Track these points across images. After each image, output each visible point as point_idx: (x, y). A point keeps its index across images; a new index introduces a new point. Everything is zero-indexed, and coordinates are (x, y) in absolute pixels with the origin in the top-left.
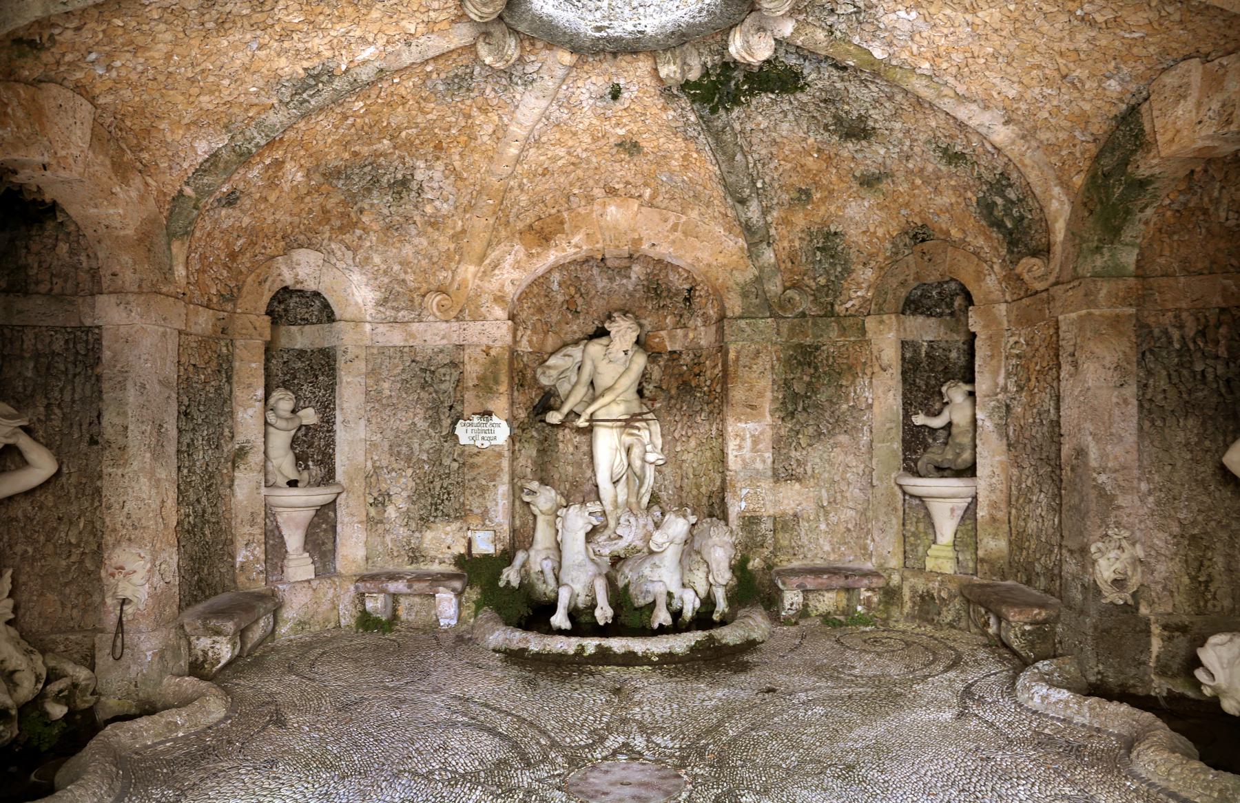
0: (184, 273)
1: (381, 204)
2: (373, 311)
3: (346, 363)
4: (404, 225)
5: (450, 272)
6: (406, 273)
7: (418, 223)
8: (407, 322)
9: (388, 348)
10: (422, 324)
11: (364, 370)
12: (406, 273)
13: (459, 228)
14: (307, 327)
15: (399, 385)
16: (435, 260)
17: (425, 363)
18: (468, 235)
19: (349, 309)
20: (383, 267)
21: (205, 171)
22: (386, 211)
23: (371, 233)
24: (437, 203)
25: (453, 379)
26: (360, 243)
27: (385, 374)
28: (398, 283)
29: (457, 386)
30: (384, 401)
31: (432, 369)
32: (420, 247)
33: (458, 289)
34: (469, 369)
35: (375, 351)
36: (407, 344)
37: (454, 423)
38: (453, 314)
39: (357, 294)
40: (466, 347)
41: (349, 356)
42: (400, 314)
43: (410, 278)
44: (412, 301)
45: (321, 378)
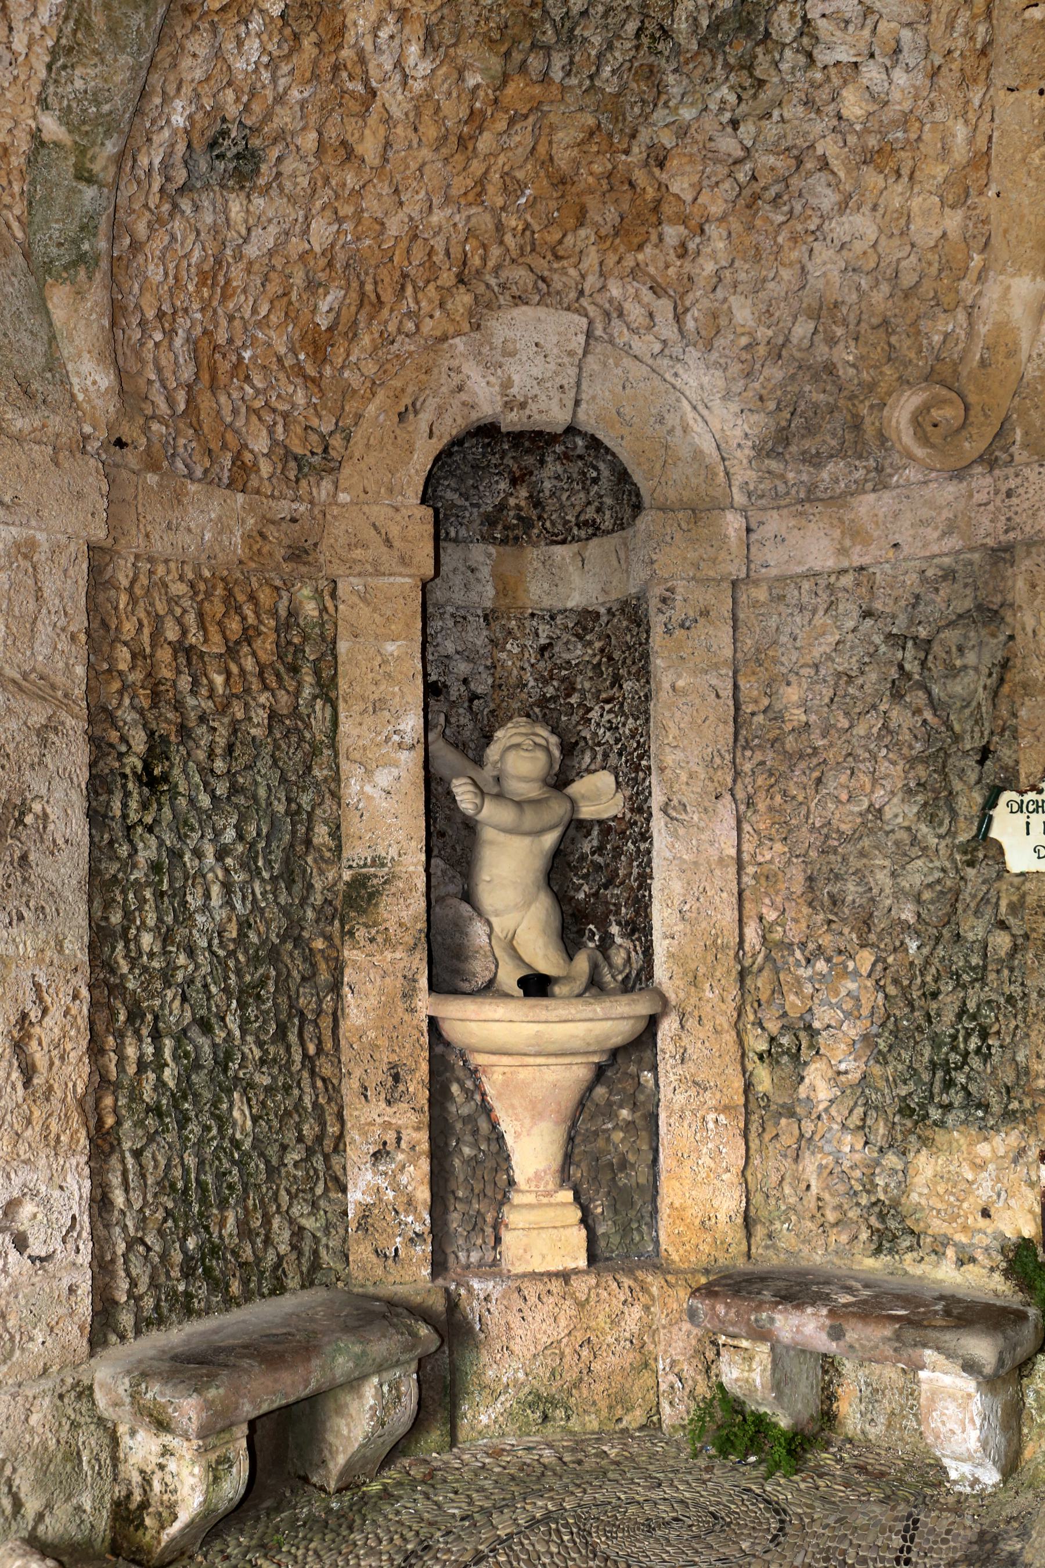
0: (105, 380)
1: (709, 124)
2: (751, 475)
3: (668, 632)
4: (795, 182)
5: (961, 316)
6: (832, 341)
7: (835, 164)
8: (843, 495)
9: (795, 579)
10: (887, 496)
11: (728, 652)
12: (832, 341)
13: (960, 153)
14: (594, 548)
15: (828, 693)
16: (908, 280)
17: (902, 619)
18: (995, 171)
19: (675, 474)
20: (763, 333)
21: (69, 51)
22: (728, 145)
23: (711, 229)
24: (872, 73)
25: (987, 660)
26: (688, 267)
27: (789, 658)
28: (816, 378)
29: (1002, 681)
30: (790, 744)
31: (923, 633)
32: (858, 247)
33: (983, 363)
34: (1030, 622)
35: (761, 594)
36: (846, 564)
37: (991, 802)
38: (972, 447)
39: (698, 427)
40: (1020, 551)
41: (678, 612)
42: (825, 475)
43: (845, 355)
44: (857, 426)
45: (627, 686)
